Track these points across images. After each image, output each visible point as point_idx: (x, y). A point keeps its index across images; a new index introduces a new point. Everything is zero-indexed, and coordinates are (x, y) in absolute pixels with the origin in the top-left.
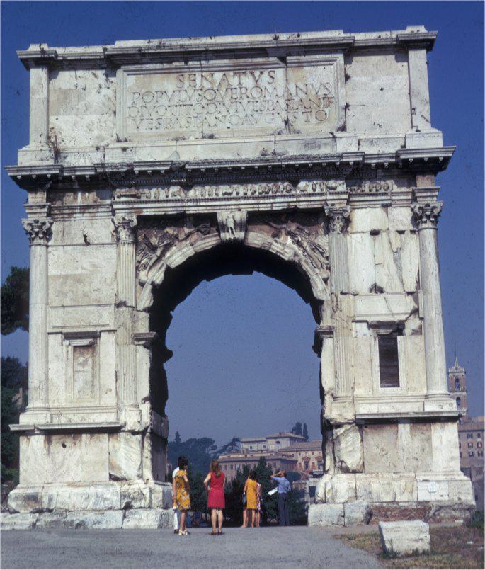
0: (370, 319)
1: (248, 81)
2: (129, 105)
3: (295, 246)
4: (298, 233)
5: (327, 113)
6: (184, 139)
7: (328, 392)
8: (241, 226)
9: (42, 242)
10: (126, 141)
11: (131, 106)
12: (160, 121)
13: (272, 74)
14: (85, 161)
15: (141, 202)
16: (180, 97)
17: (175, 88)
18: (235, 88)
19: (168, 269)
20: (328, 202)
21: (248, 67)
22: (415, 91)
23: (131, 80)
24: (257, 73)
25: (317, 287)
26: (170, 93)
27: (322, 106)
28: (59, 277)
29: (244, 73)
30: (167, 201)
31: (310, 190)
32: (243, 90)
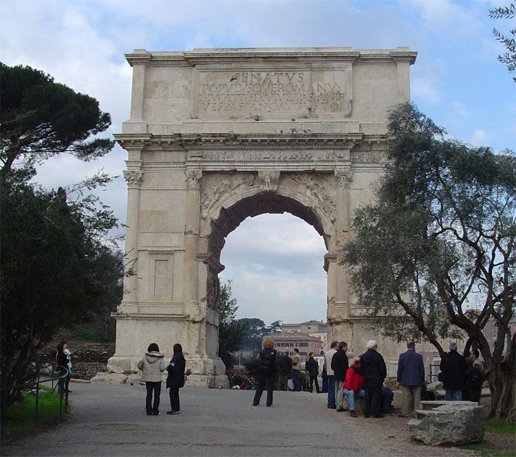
1: (284, 80)
3: (313, 197)
8: (273, 181)
10: (197, 118)
15: (207, 161)
23: (203, 75)
24: (291, 74)
31: (324, 158)
32: (281, 86)
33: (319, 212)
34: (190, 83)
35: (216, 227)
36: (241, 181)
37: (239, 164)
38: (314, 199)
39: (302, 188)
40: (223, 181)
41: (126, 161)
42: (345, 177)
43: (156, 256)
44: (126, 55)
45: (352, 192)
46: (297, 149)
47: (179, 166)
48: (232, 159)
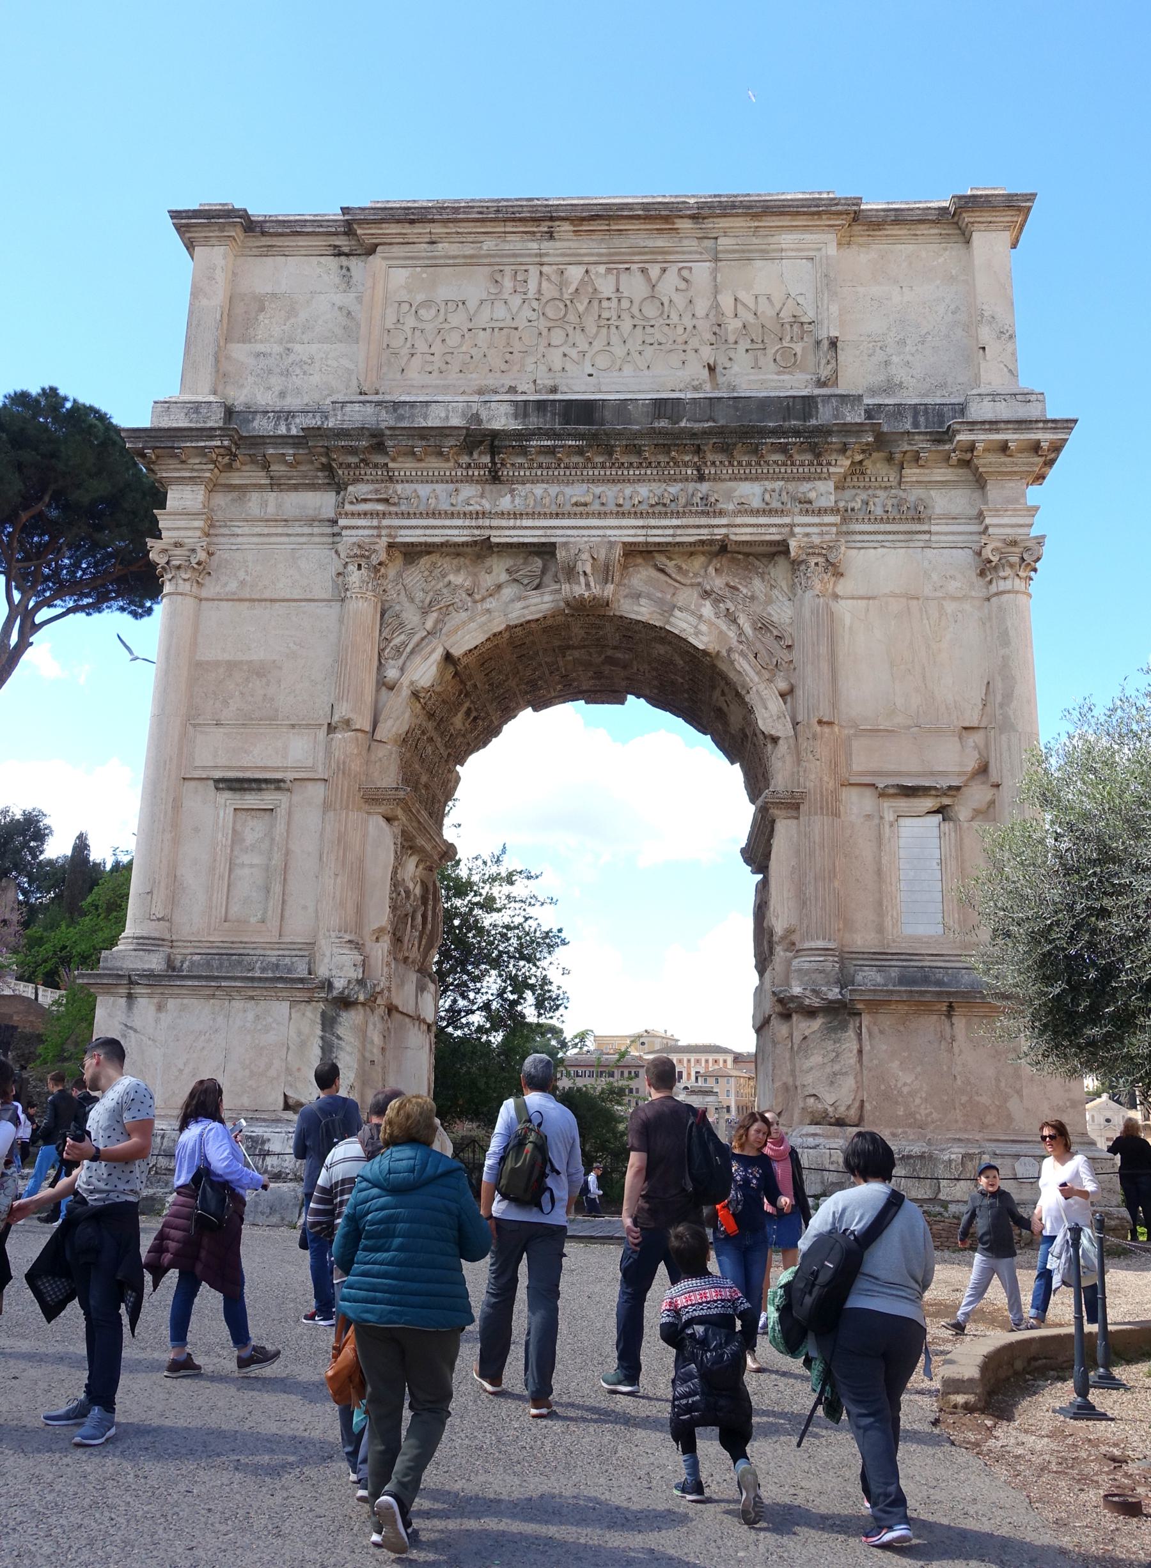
1: (634, 286)
2: (389, 325)
6: (496, 392)
7: (783, 938)
9: (185, 587)
10: (377, 394)
11: (393, 327)
12: (448, 358)
13: (685, 273)
14: (289, 429)
16: (492, 312)
18: (609, 299)
19: (448, 657)
20: (797, 530)
21: (637, 258)
22: (986, 314)
23: (400, 276)
25: (766, 708)
26: (472, 305)
27: (788, 338)
28: (217, 664)
29: (627, 269)
30: (452, 515)
31: (756, 503)
32: (625, 304)
33: (745, 669)
34: (359, 299)
35: (431, 716)
36: (504, 577)
38: (724, 628)
39: (688, 596)
40: (451, 577)
43: (237, 795)
44: (175, 215)
45: (845, 610)
46: (673, 480)
48: (478, 508)
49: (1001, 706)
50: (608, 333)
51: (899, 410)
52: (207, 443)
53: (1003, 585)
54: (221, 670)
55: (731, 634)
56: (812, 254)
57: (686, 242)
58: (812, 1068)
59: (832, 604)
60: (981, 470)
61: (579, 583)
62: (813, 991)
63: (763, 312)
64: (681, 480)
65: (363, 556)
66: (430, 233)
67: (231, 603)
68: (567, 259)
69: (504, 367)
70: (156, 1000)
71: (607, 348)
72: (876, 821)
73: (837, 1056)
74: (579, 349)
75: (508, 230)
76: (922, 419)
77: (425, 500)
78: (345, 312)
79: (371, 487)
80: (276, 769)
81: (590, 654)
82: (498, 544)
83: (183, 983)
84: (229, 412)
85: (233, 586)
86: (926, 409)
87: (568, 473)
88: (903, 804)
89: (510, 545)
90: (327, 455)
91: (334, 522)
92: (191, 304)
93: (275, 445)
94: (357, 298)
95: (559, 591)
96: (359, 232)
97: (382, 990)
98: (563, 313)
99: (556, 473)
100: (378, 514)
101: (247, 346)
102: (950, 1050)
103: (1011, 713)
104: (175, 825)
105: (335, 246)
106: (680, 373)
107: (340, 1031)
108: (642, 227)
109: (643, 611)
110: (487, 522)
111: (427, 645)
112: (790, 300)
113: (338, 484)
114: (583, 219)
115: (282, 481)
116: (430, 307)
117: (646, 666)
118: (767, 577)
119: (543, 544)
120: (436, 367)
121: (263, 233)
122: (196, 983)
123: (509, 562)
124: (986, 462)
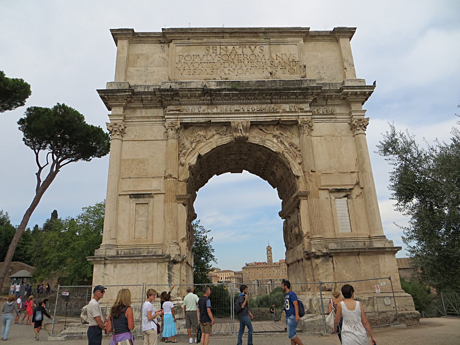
0: (330, 188)
1: (247, 51)
3: (280, 144)
4: (281, 136)
5: (295, 69)
7: (306, 235)
8: (246, 129)
9: (118, 137)
12: (195, 71)
13: (261, 48)
16: (207, 58)
17: (205, 54)
18: (240, 55)
19: (199, 156)
22: (345, 59)
23: (179, 49)
24: (253, 47)
25: (295, 168)
27: (292, 65)
28: (129, 160)
31: (288, 110)
32: (245, 56)
34: (168, 55)
35: (193, 174)
36: (215, 133)
37: (212, 116)
39: (270, 137)
40: (199, 133)
41: (109, 115)
42: (307, 125)
44: (111, 30)
46: (263, 103)
47: (158, 120)
48: (206, 112)
49: (362, 165)
50: (241, 64)
51: (325, 84)
52: (124, 94)
53: (358, 132)
54: (130, 162)
55: (283, 147)
56: (296, 43)
57: (261, 40)
58: (320, 274)
59: (311, 138)
60: (349, 100)
61: (239, 133)
62: (319, 250)
63: (284, 59)
64: (266, 104)
65: (173, 126)
66: (188, 36)
67: (132, 142)
68: (228, 44)
69: (212, 73)
70: (113, 265)
71: (241, 68)
72: (329, 199)
73: (327, 270)
74: (233, 68)
75: (211, 35)
76: (331, 87)
77: (191, 110)
78: (163, 59)
79: (174, 107)
80: (149, 191)
81: (237, 156)
82: (213, 122)
83: (123, 259)
84: (130, 87)
85: (133, 137)
86: (332, 84)
87: (233, 102)
88: (337, 195)
89: (216, 123)
90: (161, 97)
91: (163, 117)
92: (117, 56)
93: (146, 95)
94: (167, 55)
95: (233, 135)
96: (167, 36)
97: (186, 257)
98: (227, 58)
99: (230, 102)
100: (177, 114)
101: (134, 68)
102: (360, 266)
103: (365, 167)
104: (117, 209)
105: (160, 40)
106: (262, 75)
107: (174, 271)
108: (249, 35)
109: (256, 141)
110: (210, 116)
111: (193, 152)
112: (291, 55)
113: (164, 106)
114: (232, 33)
115: (147, 106)
116: (189, 57)
117: (252, 160)
118: (291, 131)
119: (226, 122)
120: (191, 73)
121: (138, 37)
122: (127, 258)
123: (216, 128)
124: (351, 98)
